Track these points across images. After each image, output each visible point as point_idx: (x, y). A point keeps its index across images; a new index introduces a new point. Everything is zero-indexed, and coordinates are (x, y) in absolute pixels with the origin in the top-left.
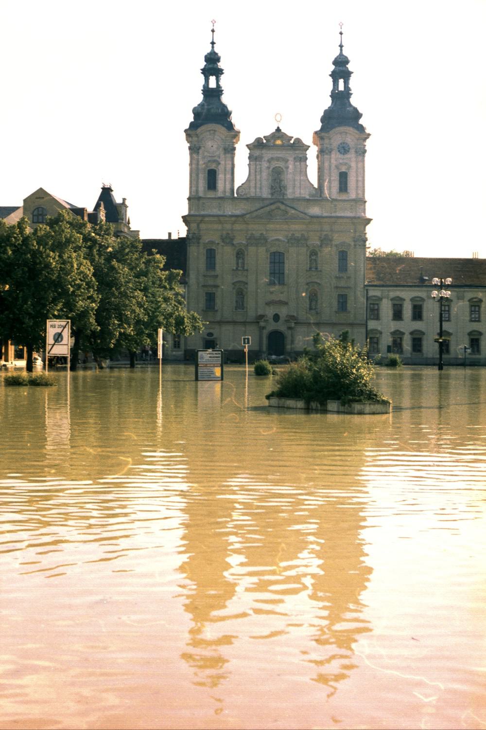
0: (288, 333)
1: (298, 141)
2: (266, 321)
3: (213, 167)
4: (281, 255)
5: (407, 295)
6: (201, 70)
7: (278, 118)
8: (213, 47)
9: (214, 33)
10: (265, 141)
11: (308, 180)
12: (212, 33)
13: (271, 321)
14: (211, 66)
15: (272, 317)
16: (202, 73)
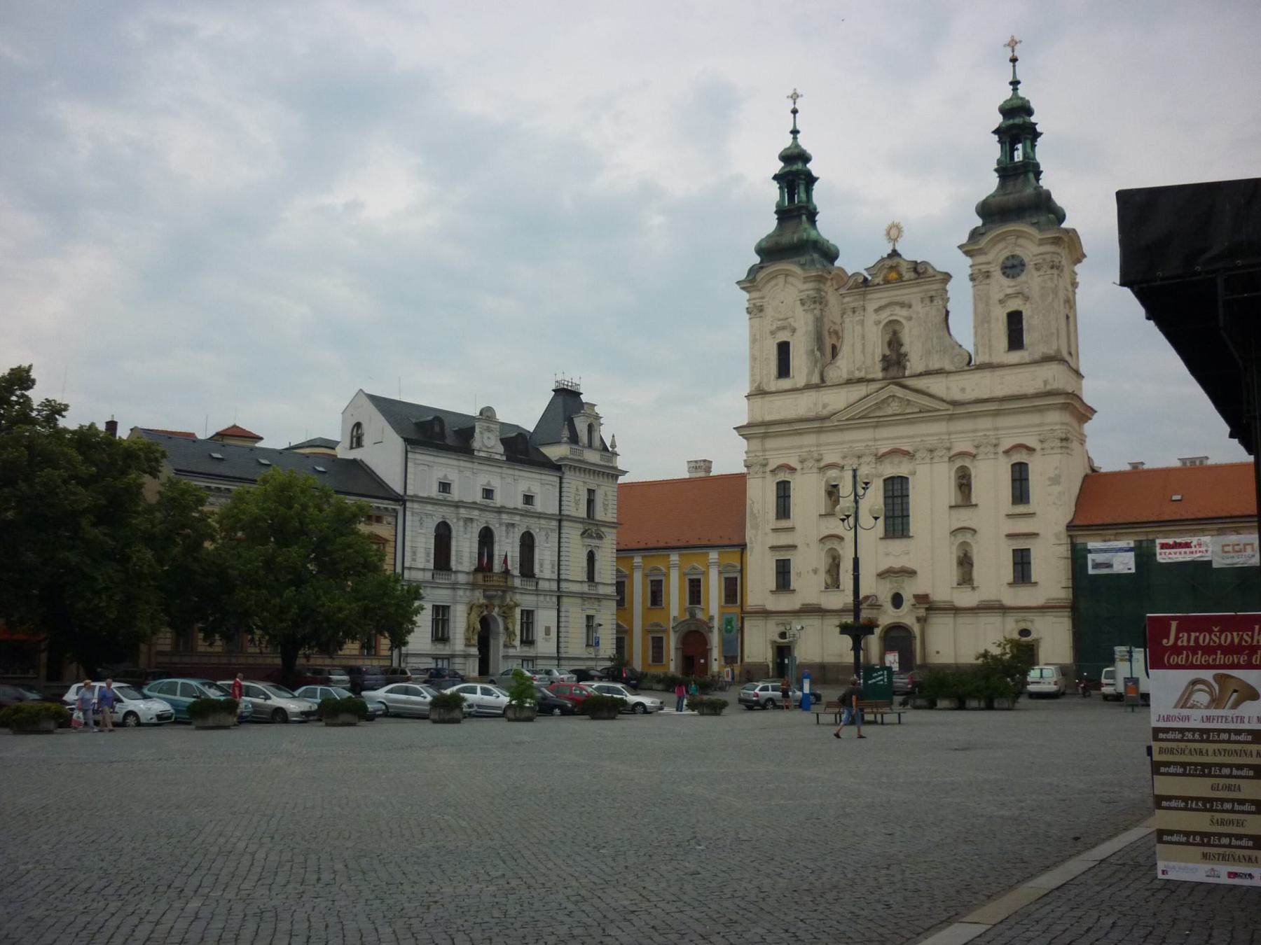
0: (916, 629)
2: (876, 606)
3: (783, 336)
4: (903, 480)
7: (894, 233)
8: (795, 138)
9: (797, 115)
10: (870, 278)
12: (792, 115)
14: (788, 169)
15: (889, 599)
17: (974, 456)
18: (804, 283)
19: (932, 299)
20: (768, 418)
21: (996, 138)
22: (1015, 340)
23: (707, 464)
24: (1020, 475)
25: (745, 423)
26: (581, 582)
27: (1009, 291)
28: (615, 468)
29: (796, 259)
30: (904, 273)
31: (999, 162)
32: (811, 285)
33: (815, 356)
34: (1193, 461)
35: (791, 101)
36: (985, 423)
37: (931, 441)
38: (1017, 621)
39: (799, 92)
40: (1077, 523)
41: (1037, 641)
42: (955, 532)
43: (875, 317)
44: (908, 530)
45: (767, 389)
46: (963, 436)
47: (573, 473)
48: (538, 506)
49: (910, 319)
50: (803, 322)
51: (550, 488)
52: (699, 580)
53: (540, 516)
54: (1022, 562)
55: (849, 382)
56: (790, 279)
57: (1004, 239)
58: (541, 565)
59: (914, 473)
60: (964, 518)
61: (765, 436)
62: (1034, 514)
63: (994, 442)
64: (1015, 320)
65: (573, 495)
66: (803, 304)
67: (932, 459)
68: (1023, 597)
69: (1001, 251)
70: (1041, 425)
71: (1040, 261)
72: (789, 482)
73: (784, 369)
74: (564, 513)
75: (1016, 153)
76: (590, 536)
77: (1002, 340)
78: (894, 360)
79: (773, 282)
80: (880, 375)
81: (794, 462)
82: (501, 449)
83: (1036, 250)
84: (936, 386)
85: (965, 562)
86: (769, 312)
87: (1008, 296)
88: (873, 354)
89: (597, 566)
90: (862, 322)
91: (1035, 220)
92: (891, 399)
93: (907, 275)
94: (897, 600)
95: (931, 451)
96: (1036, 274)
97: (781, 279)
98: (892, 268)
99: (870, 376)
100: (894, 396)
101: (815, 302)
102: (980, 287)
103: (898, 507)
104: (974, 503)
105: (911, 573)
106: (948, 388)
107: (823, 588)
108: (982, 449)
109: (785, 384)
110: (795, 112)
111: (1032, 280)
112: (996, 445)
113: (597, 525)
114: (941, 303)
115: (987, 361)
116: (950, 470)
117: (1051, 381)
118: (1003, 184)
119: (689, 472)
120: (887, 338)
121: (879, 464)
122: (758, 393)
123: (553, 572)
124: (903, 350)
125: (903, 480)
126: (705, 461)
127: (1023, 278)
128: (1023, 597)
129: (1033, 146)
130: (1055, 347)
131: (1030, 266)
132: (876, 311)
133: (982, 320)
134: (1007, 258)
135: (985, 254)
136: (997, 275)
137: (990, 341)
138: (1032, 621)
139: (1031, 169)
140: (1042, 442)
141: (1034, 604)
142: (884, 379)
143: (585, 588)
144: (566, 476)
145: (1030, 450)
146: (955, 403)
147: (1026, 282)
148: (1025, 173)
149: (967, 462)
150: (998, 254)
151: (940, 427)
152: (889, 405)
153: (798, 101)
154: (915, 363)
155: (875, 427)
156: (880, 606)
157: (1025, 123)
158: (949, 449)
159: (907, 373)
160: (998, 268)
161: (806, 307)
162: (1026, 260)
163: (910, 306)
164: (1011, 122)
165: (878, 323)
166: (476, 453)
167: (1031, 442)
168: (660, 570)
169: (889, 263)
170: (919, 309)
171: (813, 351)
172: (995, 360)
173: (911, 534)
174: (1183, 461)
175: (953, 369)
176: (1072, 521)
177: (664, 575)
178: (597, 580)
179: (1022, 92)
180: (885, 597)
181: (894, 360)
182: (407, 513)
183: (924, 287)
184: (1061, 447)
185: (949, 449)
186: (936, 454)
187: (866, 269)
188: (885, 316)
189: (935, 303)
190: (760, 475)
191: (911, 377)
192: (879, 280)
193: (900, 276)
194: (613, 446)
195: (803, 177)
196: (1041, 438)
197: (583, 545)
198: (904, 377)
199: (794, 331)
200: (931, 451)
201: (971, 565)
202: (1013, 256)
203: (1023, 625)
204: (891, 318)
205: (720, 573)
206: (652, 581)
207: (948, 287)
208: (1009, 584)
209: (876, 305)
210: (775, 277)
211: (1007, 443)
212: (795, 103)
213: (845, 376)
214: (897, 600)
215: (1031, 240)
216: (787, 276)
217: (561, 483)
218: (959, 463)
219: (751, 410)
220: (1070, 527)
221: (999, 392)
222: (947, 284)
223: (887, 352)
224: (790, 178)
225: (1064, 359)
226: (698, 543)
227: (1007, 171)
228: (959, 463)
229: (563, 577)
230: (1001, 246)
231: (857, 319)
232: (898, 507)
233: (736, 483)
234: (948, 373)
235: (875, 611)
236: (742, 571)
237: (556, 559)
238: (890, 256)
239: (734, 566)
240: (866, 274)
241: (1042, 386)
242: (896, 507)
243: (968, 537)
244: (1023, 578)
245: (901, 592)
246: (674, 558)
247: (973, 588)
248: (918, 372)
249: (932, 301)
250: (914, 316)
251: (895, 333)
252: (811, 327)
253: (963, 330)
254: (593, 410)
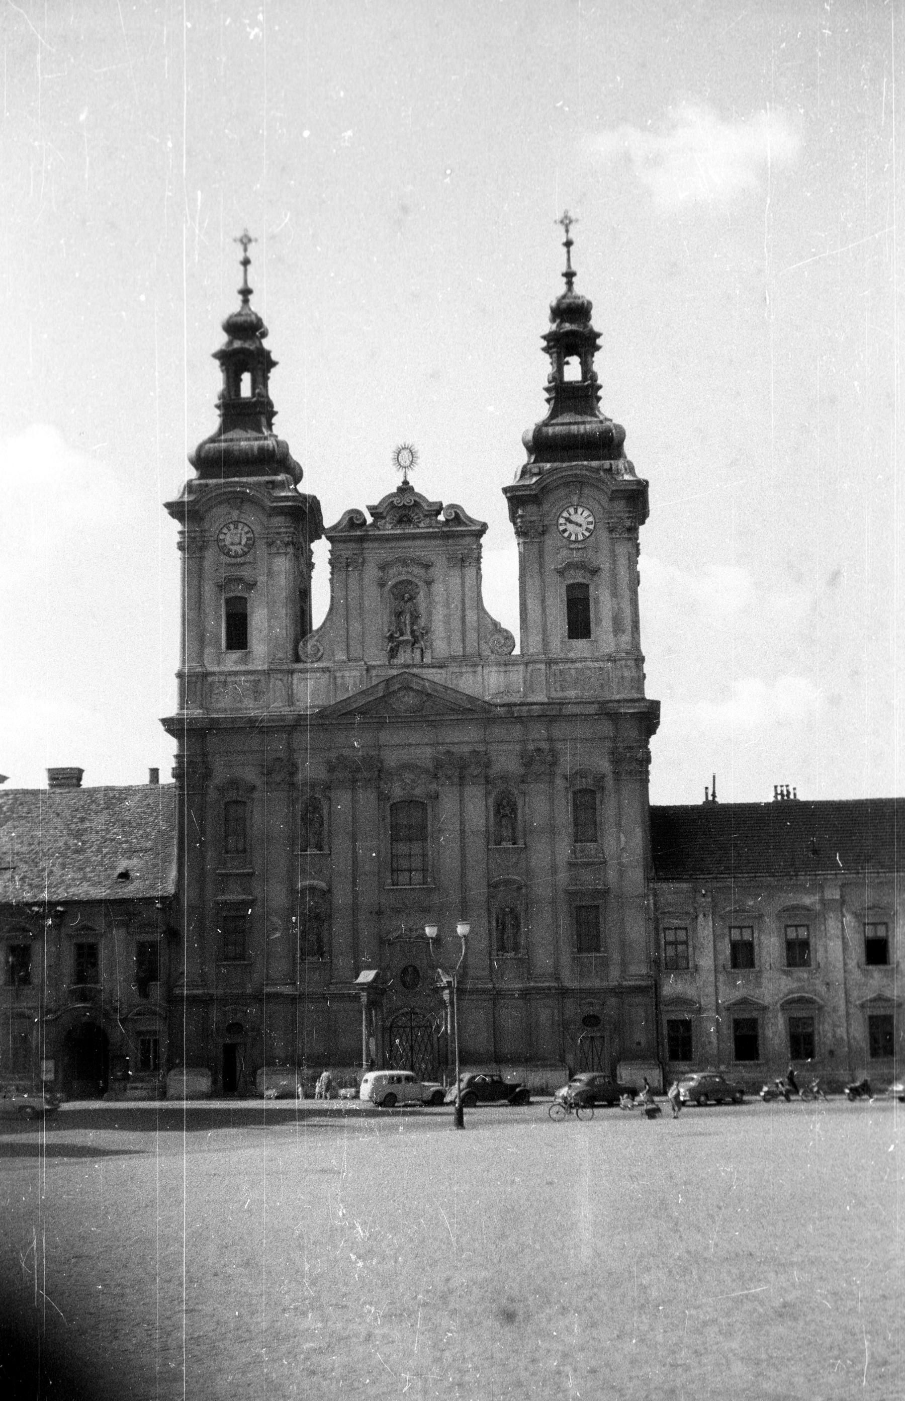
1: (458, 516)
6: (544, 337)
7: (405, 457)
10: (370, 520)
11: (331, 609)
14: (237, 344)
16: (546, 350)
35: (240, 248)
75: (566, 368)
110: (246, 262)
188: (395, 575)
222: (481, 536)
224: (242, 356)
238: (400, 489)
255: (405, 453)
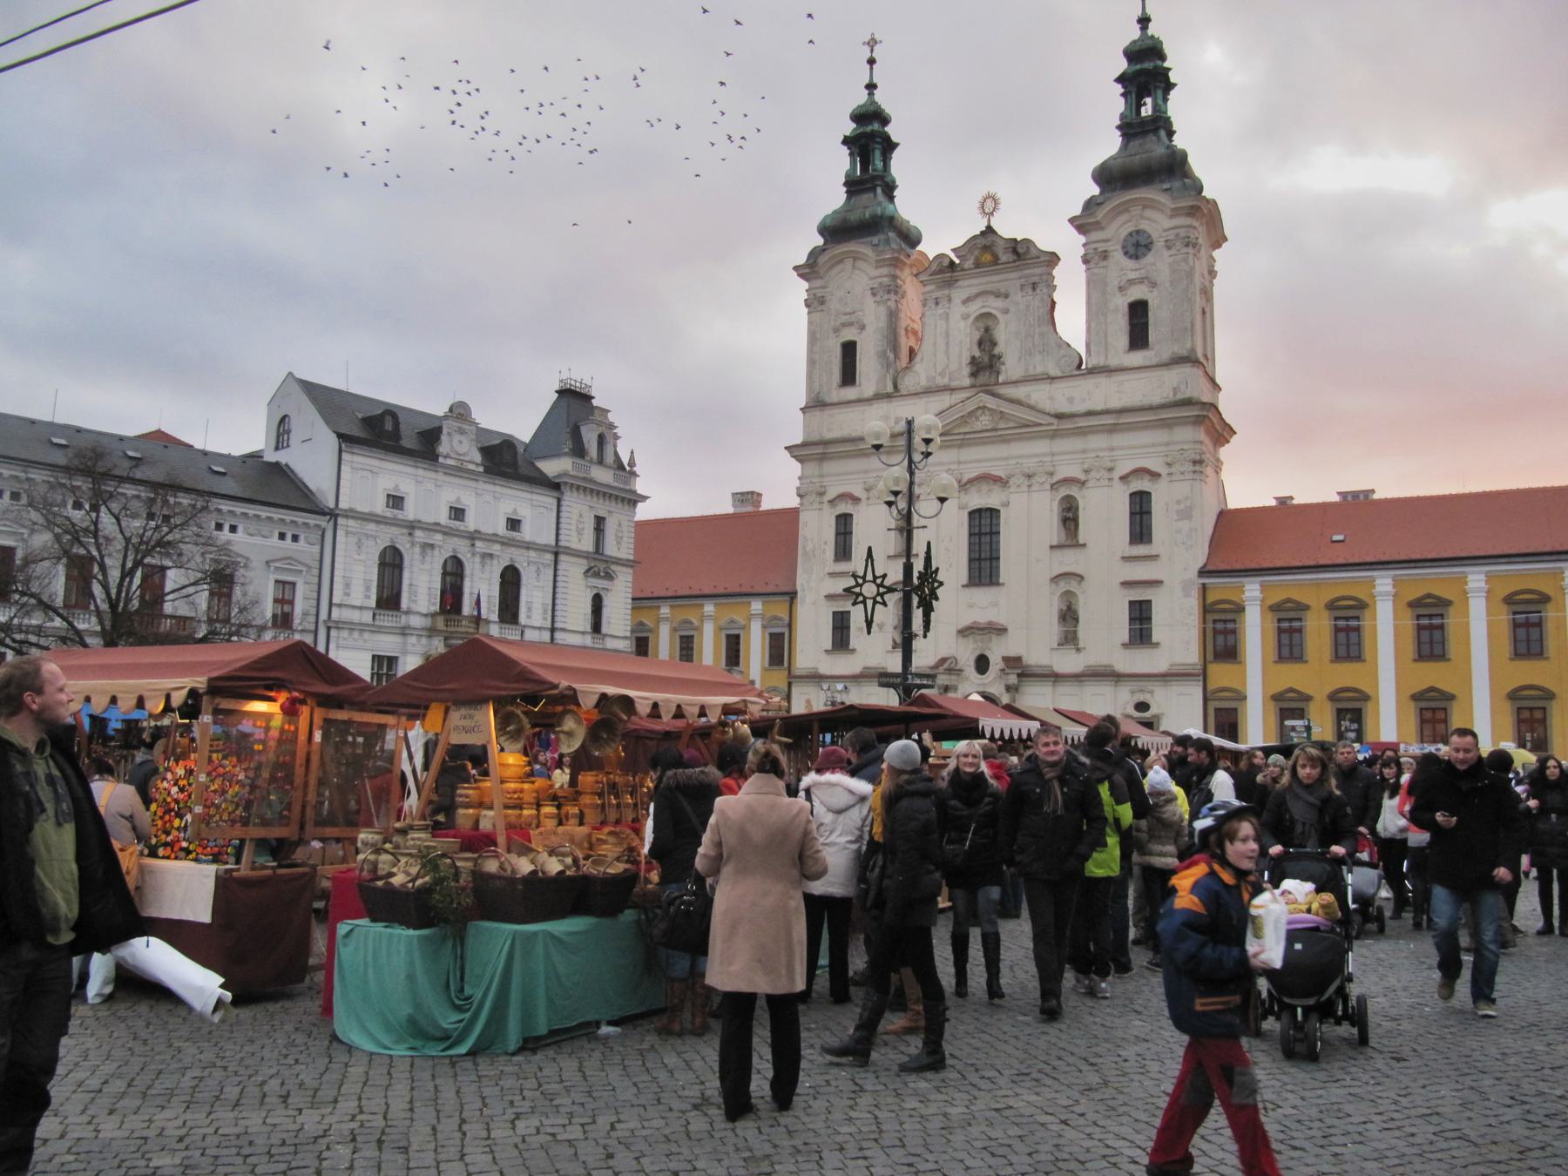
2: (954, 671)
3: (849, 335)
4: (993, 513)
5: (1315, 591)
7: (989, 205)
8: (871, 94)
10: (957, 261)
13: (971, 671)
15: (972, 663)
17: (1083, 483)
18: (877, 267)
19: (1034, 286)
20: (829, 436)
21: (1119, 89)
22: (1139, 336)
23: (752, 497)
24: (1140, 507)
25: (799, 441)
26: (583, 633)
27: (1132, 275)
28: (634, 492)
29: (869, 239)
30: (1001, 255)
31: (1122, 116)
32: (885, 271)
33: (888, 358)
34: (1355, 495)
35: (868, 49)
36: (1097, 442)
37: (1030, 465)
38: (1133, 692)
39: (877, 37)
40: (1209, 568)
41: (1157, 717)
42: (1056, 579)
43: (964, 309)
44: (998, 575)
45: (828, 400)
46: (1068, 457)
47: (575, 494)
48: (527, 533)
49: (1006, 311)
50: (873, 316)
51: (544, 511)
52: (737, 637)
53: (528, 546)
54: (1140, 615)
55: (928, 392)
56: (859, 264)
57: (1127, 210)
58: (529, 609)
59: (1006, 504)
60: (1069, 561)
61: (823, 458)
62: (1157, 556)
63: (1109, 465)
64: (1138, 311)
65: (574, 522)
66: (874, 295)
67: (1029, 486)
68: (1141, 661)
69: (1120, 227)
70: (1167, 444)
71: (1172, 237)
72: (851, 515)
73: (849, 376)
74: (562, 543)
76: (597, 575)
77: (1122, 340)
78: (985, 364)
79: (839, 267)
80: (967, 382)
81: (858, 491)
82: (478, 458)
83: (1168, 223)
84: (1039, 395)
85: (1069, 616)
86: (833, 304)
87: (1131, 282)
88: (960, 356)
89: (606, 612)
90: (947, 317)
91: (1166, 186)
92: (980, 412)
93: (1004, 258)
94: (982, 664)
95: (1029, 477)
96: (1166, 253)
97: (849, 262)
98: (986, 248)
99: (955, 384)
100: (984, 408)
101: (889, 292)
102: (1096, 271)
103: (986, 548)
104: (1081, 542)
105: (1001, 631)
106: (1052, 398)
107: (890, 648)
108: (1093, 474)
109: (850, 393)
110: (871, 62)
111: (1160, 262)
112: (1111, 470)
113: (606, 562)
114: (1045, 290)
115: (1102, 364)
116: (1052, 500)
117: (1183, 387)
118: (1125, 146)
119: (734, 506)
120: (977, 336)
121: (963, 493)
122: (816, 404)
123: (545, 619)
124: (996, 351)
125: (993, 513)
126: (753, 493)
127: (1149, 258)
128: (1141, 661)
129: (1165, 100)
130: (1189, 345)
131: (1159, 244)
132: (965, 302)
133: (1095, 313)
134: (1131, 234)
135: (1103, 229)
136: (1118, 256)
137: (1106, 337)
138: (1151, 692)
139: (1161, 125)
140: (1169, 465)
141: (1155, 671)
142: (973, 386)
143: (588, 641)
144: (565, 497)
145: (1155, 476)
146: (1060, 416)
147: (1154, 264)
148: (1155, 131)
149: (1074, 491)
150: (1118, 230)
151: (1041, 446)
152: (977, 419)
153: (876, 48)
154: (1012, 367)
155: (960, 446)
156: (961, 670)
157: (1156, 67)
158: (1051, 474)
159: (1001, 380)
160: (1119, 247)
161: (878, 298)
162: (1154, 236)
163: (1007, 296)
164: (1138, 67)
165: (965, 317)
166: (441, 460)
167: (1154, 464)
168: (692, 623)
169: (982, 241)
170: (1017, 297)
171: (884, 353)
172: (1114, 362)
173: (1001, 581)
174: (1343, 494)
175: (1060, 374)
176: (1205, 565)
177: (696, 629)
178: (604, 630)
179: (1152, 30)
180: (967, 659)
181: (985, 364)
182: (339, 532)
183: (1026, 272)
184: (1194, 472)
185: (1051, 474)
186: (1033, 481)
187: (954, 250)
188: (975, 308)
189: (1038, 291)
190: (816, 506)
191: (1004, 383)
192: (969, 264)
193: (996, 260)
194: (632, 463)
195: (879, 140)
196: (1169, 460)
197: (587, 587)
198: (997, 383)
199: (863, 328)
200: (1029, 477)
201: (1077, 620)
202: (1138, 232)
203: (1141, 698)
204: (983, 310)
205: (764, 627)
206: (681, 637)
207: (1055, 272)
208: (1124, 645)
209: (964, 294)
210: (841, 261)
211: (1125, 467)
212: (872, 51)
213: (924, 382)
214: (982, 664)
215: (1162, 211)
216: (855, 259)
217: (559, 506)
218: (1063, 492)
219: (806, 426)
220: (1203, 573)
221: (1115, 403)
223: (977, 354)
224: (863, 141)
225: (1197, 360)
226: (737, 590)
227: (1131, 128)
228: (1063, 492)
229: (558, 625)
230: (1124, 217)
231: (941, 311)
232: (986, 548)
233: (789, 517)
234: (1053, 378)
235: (954, 677)
236: (790, 625)
237: (550, 602)
238: (983, 233)
239: (780, 619)
240: (953, 256)
241: (1171, 395)
242: (983, 548)
243: (1073, 586)
244: (1141, 636)
245: (987, 653)
246: (709, 608)
247: (1078, 650)
248: (1014, 379)
249: (1034, 289)
250: (1012, 309)
251: (987, 330)
252: (883, 322)
253: (1072, 323)
254: (606, 417)
255: (989, 201)
